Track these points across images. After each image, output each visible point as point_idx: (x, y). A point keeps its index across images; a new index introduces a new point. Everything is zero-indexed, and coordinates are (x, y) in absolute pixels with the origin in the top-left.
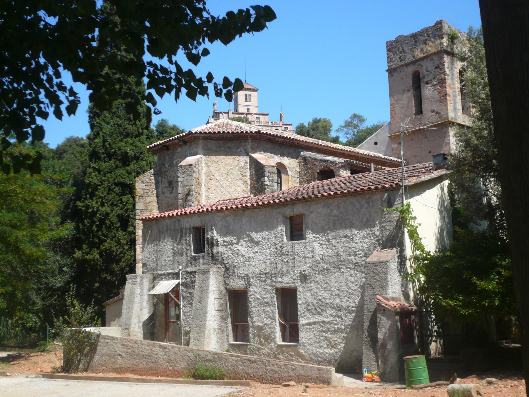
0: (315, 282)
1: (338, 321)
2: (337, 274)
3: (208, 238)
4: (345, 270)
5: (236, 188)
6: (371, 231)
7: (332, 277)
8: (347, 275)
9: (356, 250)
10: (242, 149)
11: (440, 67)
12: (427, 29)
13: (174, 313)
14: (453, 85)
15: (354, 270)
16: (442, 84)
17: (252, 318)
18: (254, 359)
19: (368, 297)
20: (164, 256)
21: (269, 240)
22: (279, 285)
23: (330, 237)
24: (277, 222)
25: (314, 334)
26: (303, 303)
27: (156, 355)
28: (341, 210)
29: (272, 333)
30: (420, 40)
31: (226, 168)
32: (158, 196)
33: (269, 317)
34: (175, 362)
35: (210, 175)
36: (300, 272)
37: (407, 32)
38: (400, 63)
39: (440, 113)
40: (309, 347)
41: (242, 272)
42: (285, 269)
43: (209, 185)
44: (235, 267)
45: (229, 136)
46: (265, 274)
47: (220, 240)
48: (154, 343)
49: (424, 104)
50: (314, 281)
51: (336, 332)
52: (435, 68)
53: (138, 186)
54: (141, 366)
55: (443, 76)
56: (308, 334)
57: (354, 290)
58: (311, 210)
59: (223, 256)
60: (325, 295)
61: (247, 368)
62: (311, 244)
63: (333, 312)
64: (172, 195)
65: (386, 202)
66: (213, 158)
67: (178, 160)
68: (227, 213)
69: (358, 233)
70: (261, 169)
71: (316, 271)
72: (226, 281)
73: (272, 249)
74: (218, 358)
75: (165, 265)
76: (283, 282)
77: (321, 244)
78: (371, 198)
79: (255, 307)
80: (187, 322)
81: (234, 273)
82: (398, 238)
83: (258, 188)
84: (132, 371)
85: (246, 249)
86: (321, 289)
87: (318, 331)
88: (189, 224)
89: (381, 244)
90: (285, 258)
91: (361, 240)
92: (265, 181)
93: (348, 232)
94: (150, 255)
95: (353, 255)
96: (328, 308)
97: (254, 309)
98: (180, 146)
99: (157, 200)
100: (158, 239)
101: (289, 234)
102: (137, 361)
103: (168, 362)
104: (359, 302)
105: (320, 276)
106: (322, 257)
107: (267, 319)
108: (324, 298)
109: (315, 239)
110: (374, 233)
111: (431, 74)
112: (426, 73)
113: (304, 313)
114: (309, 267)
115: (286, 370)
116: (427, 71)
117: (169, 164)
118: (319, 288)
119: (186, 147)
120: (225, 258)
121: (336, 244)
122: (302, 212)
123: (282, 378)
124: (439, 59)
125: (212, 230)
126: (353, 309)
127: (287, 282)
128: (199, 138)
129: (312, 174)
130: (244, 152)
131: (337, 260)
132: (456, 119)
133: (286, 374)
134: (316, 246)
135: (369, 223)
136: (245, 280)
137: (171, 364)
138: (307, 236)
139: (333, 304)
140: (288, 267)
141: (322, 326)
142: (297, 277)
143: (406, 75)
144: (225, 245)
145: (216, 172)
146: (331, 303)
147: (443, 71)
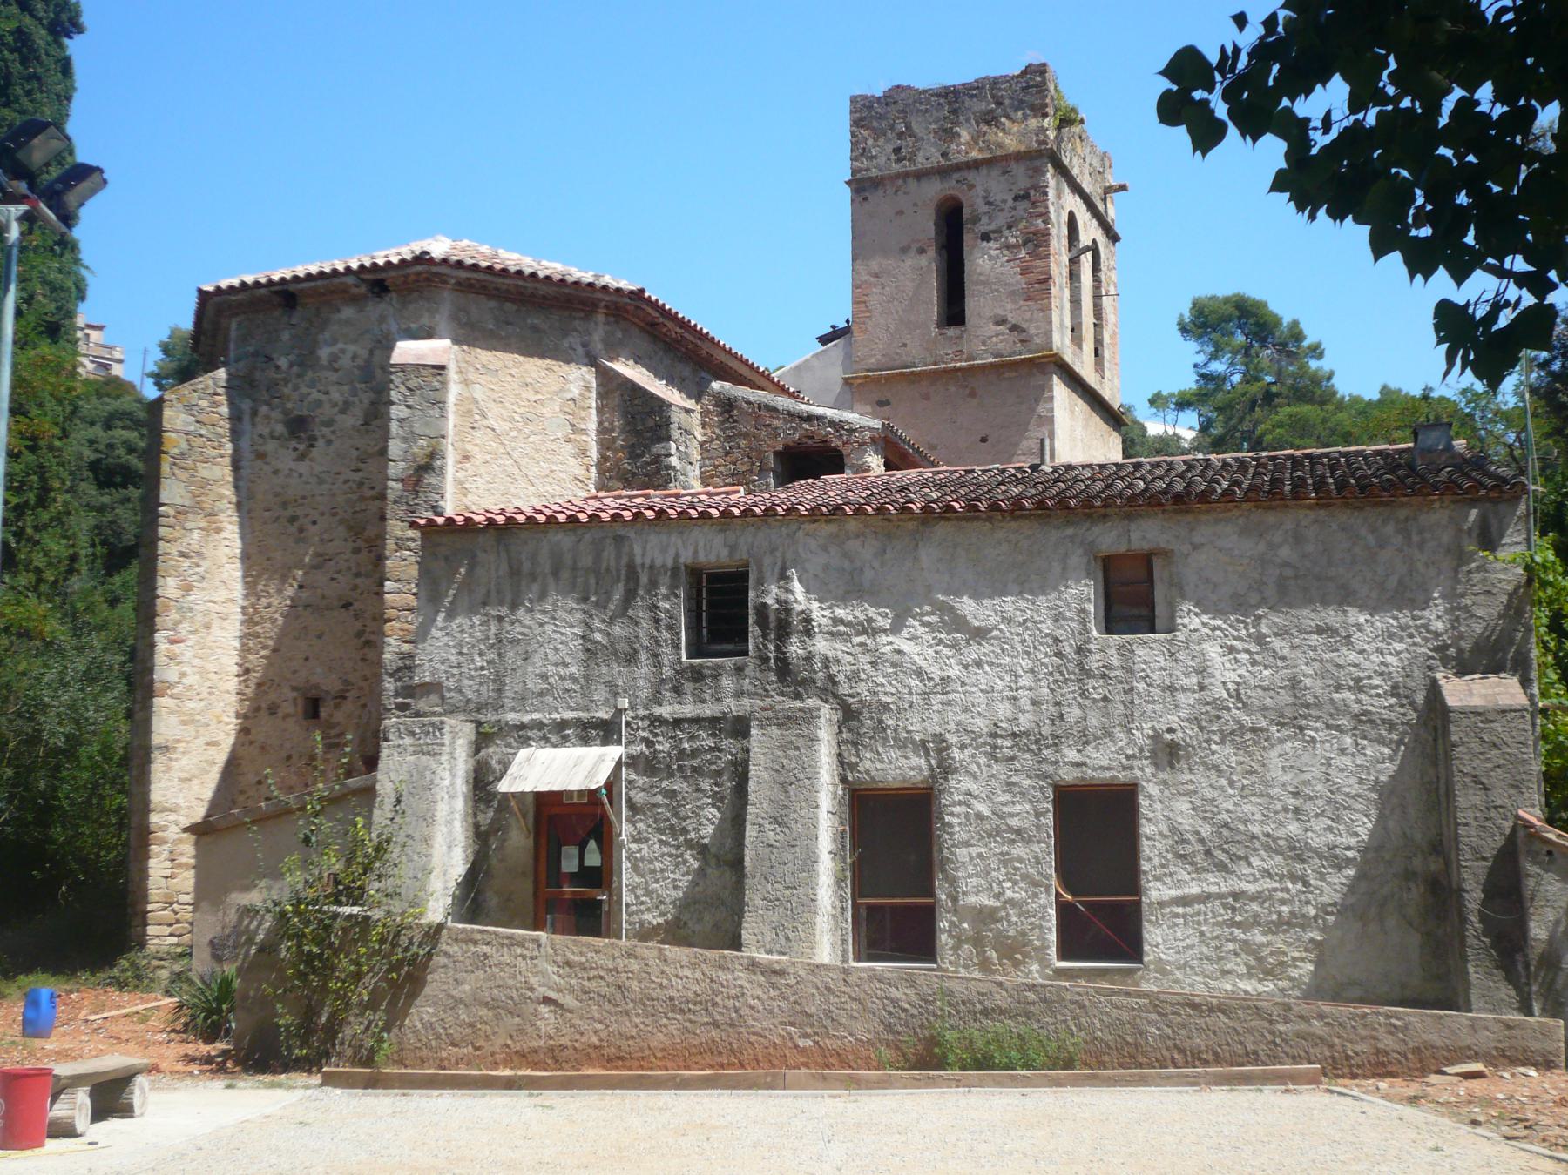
0: (1207, 767)
1: (1293, 892)
2: (1289, 744)
3: (765, 605)
4: (1321, 734)
5: (555, 468)
6: (1414, 618)
7: (1274, 753)
8: (1329, 750)
9: (1362, 675)
10: (574, 340)
11: (1032, 197)
12: (995, 82)
13: (576, 862)
15: (1354, 735)
16: (1036, 246)
17: (953, 882)
18: (1214, 1001)
19: (1470, 814)
20: (537, 659)
21: (1029, 624)
22: (1068, 775)
23: (1265, 630)
24: (1064, 569)
25: (1202, 934)
26: (1160, 833)
27: (735, 997)
28: (1309, 548)
29: (1031, 930)
30: (970, 109)
31: (524, 396)
32: (236, 465)
33: (1025, 877)
34: (827, 1023)
35: (473, 414)
36: (1151, 733)
37: (926, 79)
38: (896, 168)
40: (1179, 975)
41: (916, 725)
42: (1094, 721)
43: (469, 447)
44: (886, 707)
45: (543, 290)
46: (1014, 735)
47: (820, 615)
48: (724, 957)
49: (973, 296)
50: (1204, 764)
51: (1283, 925)
52: (1016, 199)
53: (171, 418)
54: (658, 1040)
55: (1042, 226)
56: (1179, 934)
57: (1353, 797)
58: (1197, 539)
59: (834, 670)
60: (1247, 808)
61: (1183, 1032)
62: (1192, 646)
63: (1276, 863)
64: (303, 467)
65: (1474, 535)
66: (485, 356)
67: (340, 346)
68: (852, 525)
69: (1367, 621)
70: (651, 413)
71: (1214, 733)
72: (846, 754)
73: (1041, 656)
74: (1045, 1001)
75: (542, 694)
76: (1085, 764)
77: (1231, 650)
78: (1415, 519)
79: (966, 844)
80: (649, 893)
81: (881, 727)
82: (1511, 642)
83: (634, 474)
84: (610, 1060)
85: (931, 651)
86: (1231, 792)
87: (1215, 924)
88: (672, 552)
89: (1454, 659)
90: (1094, 688)
91: (1380, 645)
92: (670, 455)
93: (1332, 617)
94: (461, 653)
95: (1350, 689)
96: (1255, 850)
97: (962, 852)
98: (355, 300)
99: (237, 479)
100: (508, 598)
101: (1102, 613)
102: (638, 1021)
103: (792, 1024)
104: (1372, 833)
105: (1228, 750)
106: (1237, 690)
107: (1015, 883)
108: (1240, 819)
109: (1207, 631)
110: (1425, 626)
111: (1006, 214)
113: (1163, 866)
114: (1189, 720)
115: (1363, 1032)
116: (989, 203)
117: (293, 358)
118: (1222, 788)
119: (383, 306)
120: (841, 678)
121: (1286, 652)
122: (1162, 545)
123: (1348, 1058)
124: (1030, 173)
125: (784, 577)
126: (1350, 854)
127: (1102, 763)
128: (445, 282)
129: (755, 454)
130: (580, 350)
131: (1290, 700)
133: (1363, 1047)
134: (1213, 655)
135: (1408, 595)
136: (927, 754)
137: (809, 1030)
138: (1179, 621)
139: (1275, 840)
140: (1107, 715)
141: (1234, 909)
142: (1141, 750)
143: (915, 205)
144: (840, 634)
145: (492, 405)
146: (1268, 835)
147: (1043, 210)
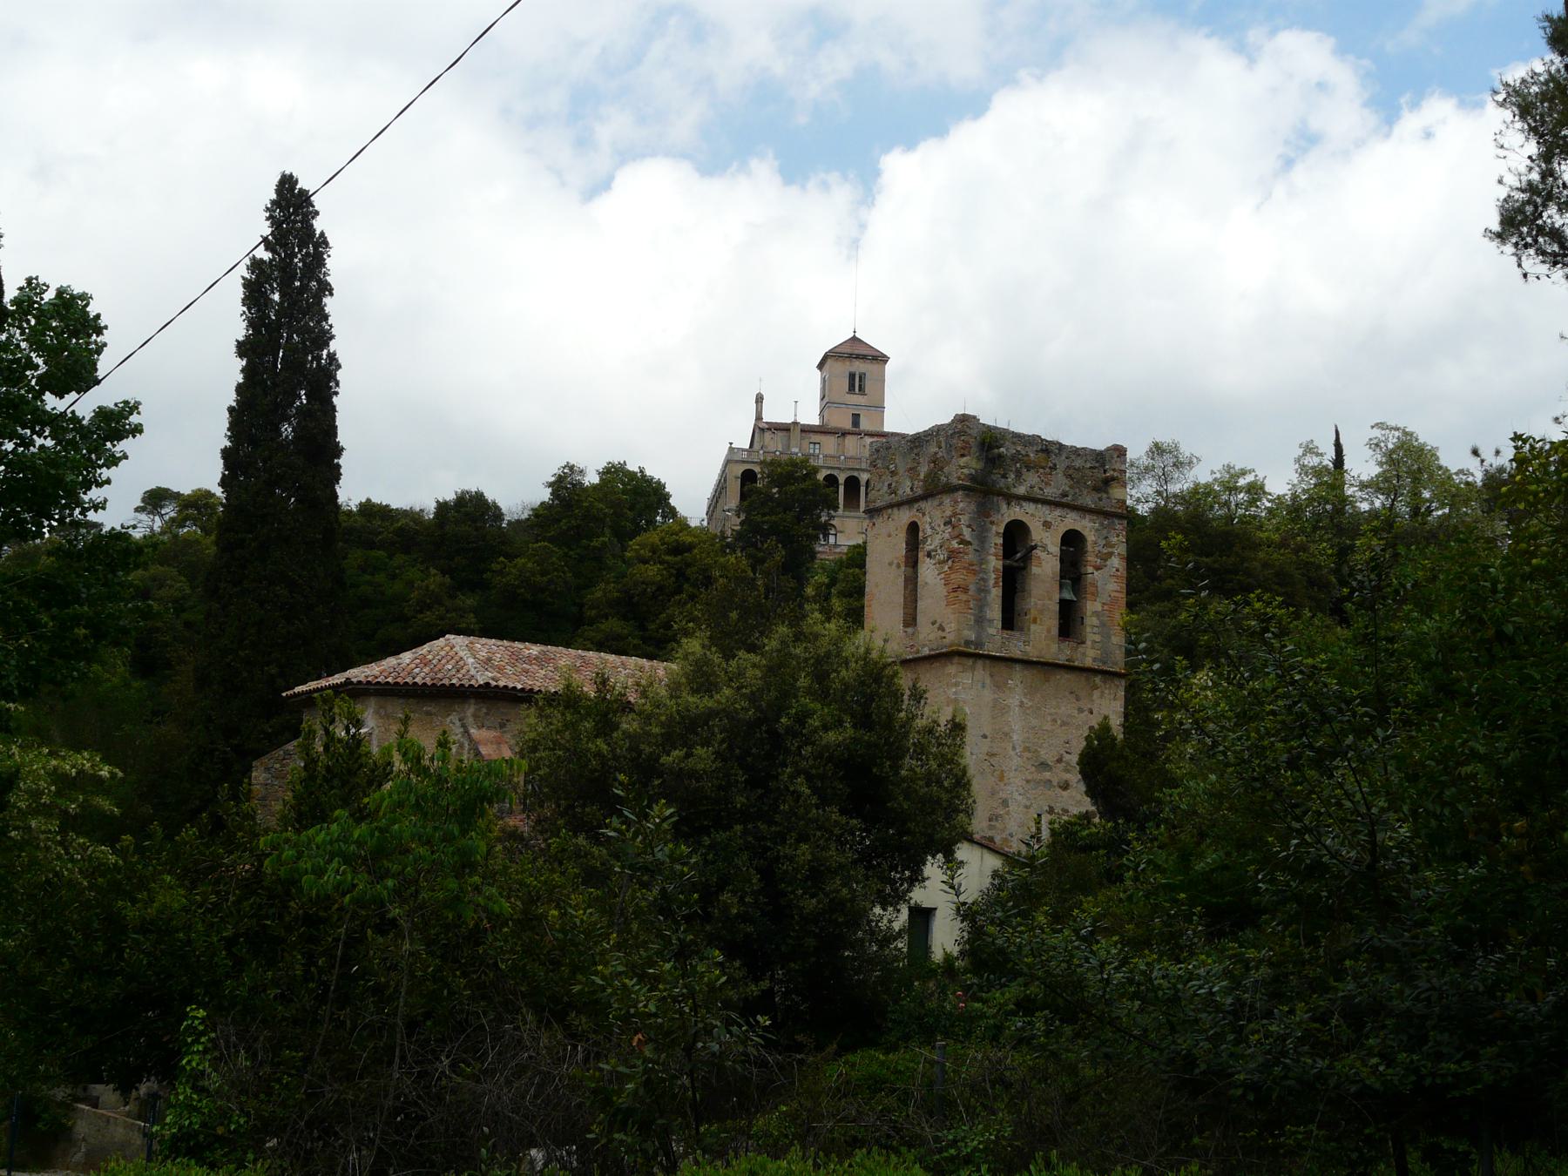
14: (981, 564)
39: (943, 630)
111: (939, 536)
112: (929, 531)
116: (932, 528)
132: (979, 644)
